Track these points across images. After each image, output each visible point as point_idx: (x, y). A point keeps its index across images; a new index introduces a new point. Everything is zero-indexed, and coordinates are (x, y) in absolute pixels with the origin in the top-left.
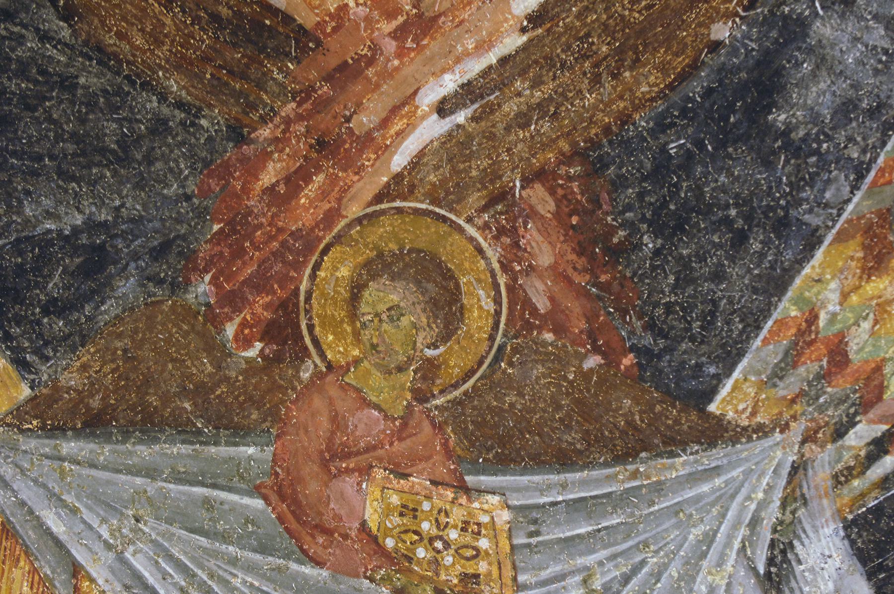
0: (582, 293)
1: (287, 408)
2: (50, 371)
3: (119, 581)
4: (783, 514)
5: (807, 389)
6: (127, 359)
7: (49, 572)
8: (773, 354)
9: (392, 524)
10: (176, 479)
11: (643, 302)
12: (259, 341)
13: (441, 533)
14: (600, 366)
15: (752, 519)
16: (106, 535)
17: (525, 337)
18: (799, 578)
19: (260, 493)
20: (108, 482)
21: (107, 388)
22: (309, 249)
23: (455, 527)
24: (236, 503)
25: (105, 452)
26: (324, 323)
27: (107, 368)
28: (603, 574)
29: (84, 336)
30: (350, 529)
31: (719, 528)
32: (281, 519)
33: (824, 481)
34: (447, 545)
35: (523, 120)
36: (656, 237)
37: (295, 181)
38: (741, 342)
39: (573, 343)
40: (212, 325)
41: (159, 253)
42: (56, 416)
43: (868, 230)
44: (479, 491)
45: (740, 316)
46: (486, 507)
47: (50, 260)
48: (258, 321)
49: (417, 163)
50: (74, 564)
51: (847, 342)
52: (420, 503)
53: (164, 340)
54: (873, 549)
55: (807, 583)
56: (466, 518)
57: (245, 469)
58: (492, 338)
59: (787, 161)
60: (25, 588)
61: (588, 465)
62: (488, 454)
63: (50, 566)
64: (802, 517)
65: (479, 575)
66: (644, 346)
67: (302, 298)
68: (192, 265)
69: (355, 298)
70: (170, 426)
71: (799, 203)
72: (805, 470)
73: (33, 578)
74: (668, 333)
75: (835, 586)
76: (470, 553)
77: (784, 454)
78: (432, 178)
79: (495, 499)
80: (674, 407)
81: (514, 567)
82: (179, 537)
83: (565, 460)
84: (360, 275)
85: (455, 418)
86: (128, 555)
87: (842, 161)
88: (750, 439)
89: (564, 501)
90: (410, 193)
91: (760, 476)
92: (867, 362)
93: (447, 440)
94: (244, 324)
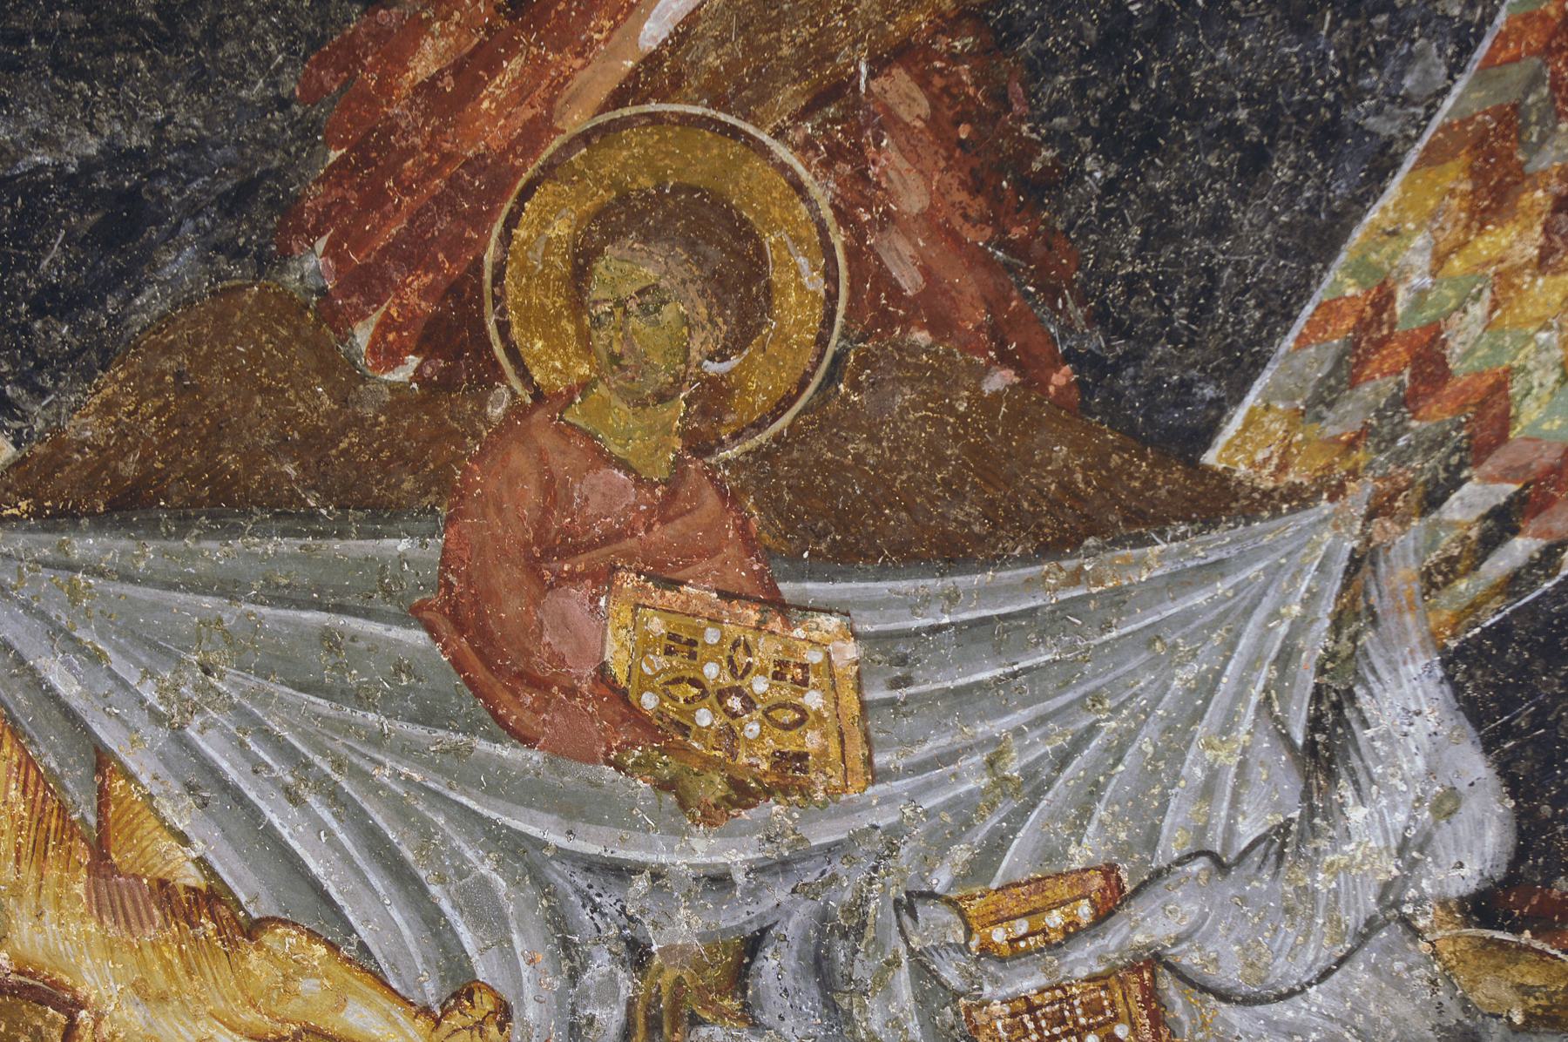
0: (978, 260)
1: (465, 469)
2: (49, 414)
3: (176, 777)
4: (1336, 642)
5: (1375, 422)
6: (182, 391)
7: (53, 765)
8: (1316, 363)
9: (653, 669)
10: (272, 598)
11: (1086, 275)
12: (415, 353)
13: (738, 683)
14: (1013, 387)
15: (1282, 651)
16: (152, 697)
17: (880, 338)
18: (1364, 750)
19: (420, 620)
20: (154, 606)
21: (148, 441)
22: (498, 189)
23: (763, 671)
24: (378, 638)
25: (149, 553)
26: (527, 320)
27: (149, 407)
28: (1022, 750)
29: (107, 350)
30: (579, 678)
31: (1224, 667)
32: (458, 664)
33: (1407, 582)
34: (749, 703)
36: (1108, 160)
37: (472, 69)
38: (1259, 343)
39: (964, 349)
40: (331, 327)
41: (235, 203)
42: (61, 492)
44: (805, 609)
45: (1256, 297)
46: (816, 636)
47: (43, 218)
48: (410, 317)
49: (686, 34)
50: (97, 750)
51: (1445, 340)
52: (701, 631)
53: (248, 356)
54: (1492, 699)
55: (1378, 760)
56: (781, 657)
57: (394, 577)
58: (822, 341)
59: (1336, 23)
60: (13, 793)
61: (995, 561)
62: (818, 544)
63: (56, 754)
64: (1368, 645)
65: (806, 755)
66: (1089, 351)
67: (487, 277)
68: (292, 223)
69: (580, 274)
70: (259, 505)
71: (1358, 96)
72: (1374, 563)
73: (26, 774)
74: (1131, 327)
75: (1428, 763)
76: (789, 716)
77: (1336, 536)
78: (712, 60)
79: (832, 623)
80: (1143, 457)
81: (868, 741)
82: (280, 698)
84: (589, 233)
85: (760, 481)
86: (191, 732)
87: (1434, 22)
88: (1276, 513)
89: (952, 624)
90: (673, 88)
91: (1294, 577)
92: (1480, 374)
93: (746, 521)
94: (386, 325)
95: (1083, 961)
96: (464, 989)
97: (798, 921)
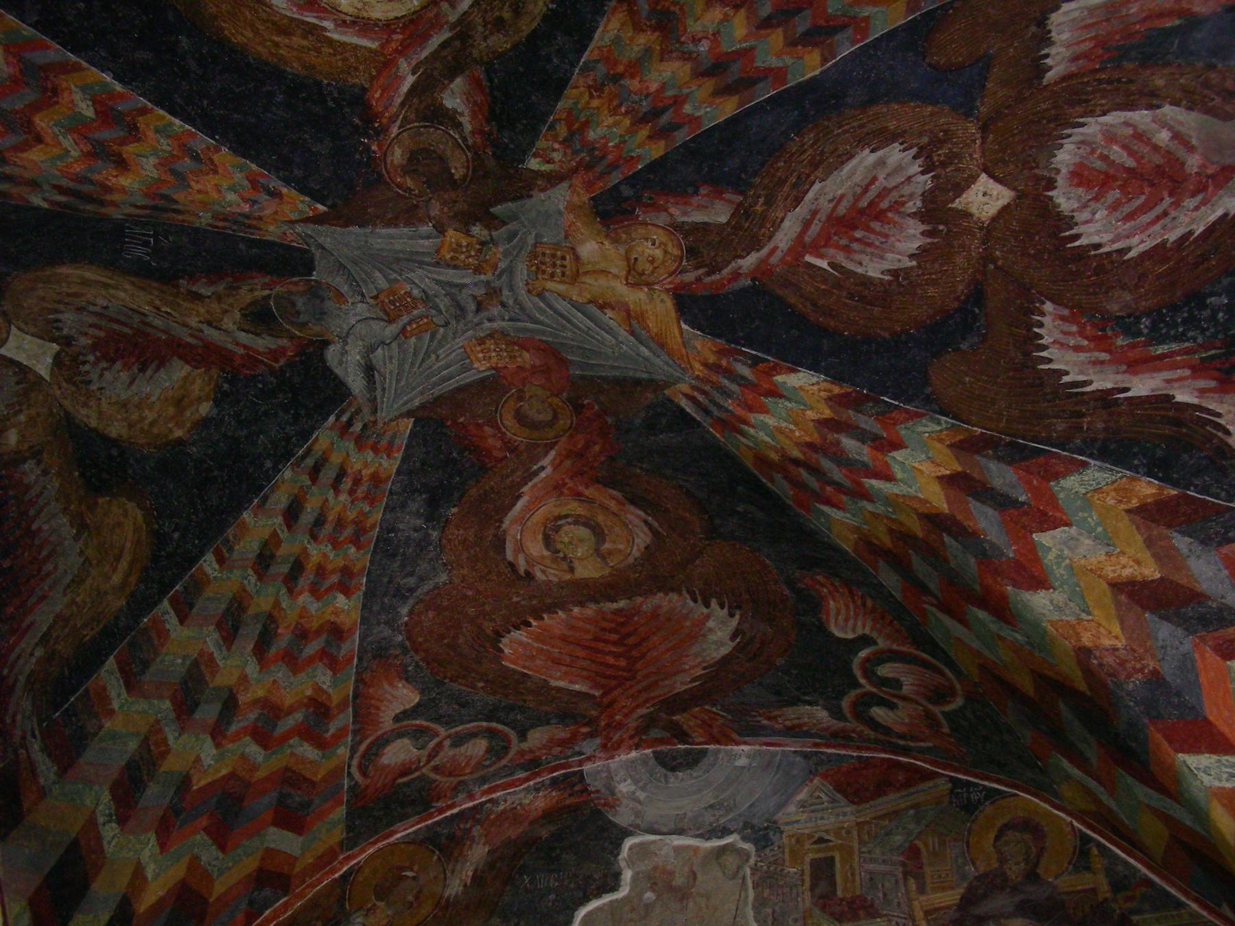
8: (398, 442)
25: (631, 373)
35: (513, 471)
37: (587, 447)
43: (381, 482)
83: (460, 389)
90: (546, 445)
95: (405, 319)
96: (540, 295)
97: (470, 316)
